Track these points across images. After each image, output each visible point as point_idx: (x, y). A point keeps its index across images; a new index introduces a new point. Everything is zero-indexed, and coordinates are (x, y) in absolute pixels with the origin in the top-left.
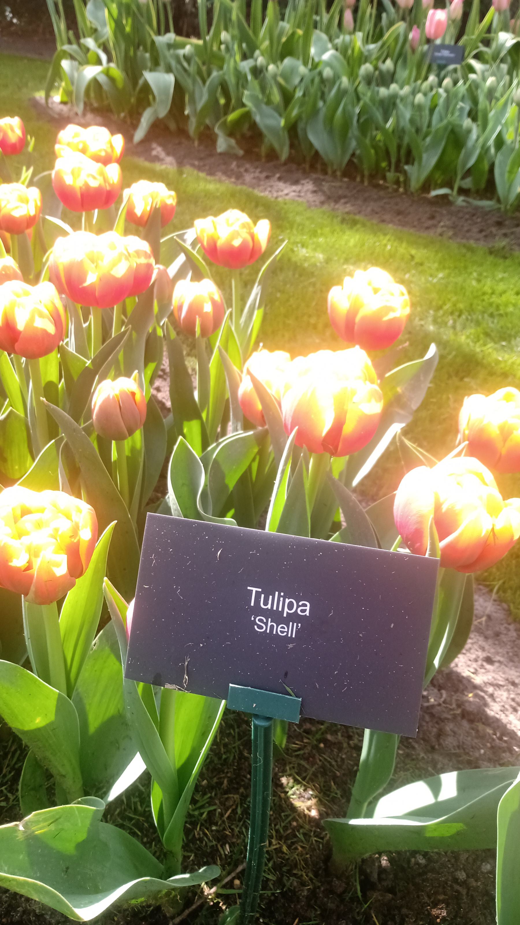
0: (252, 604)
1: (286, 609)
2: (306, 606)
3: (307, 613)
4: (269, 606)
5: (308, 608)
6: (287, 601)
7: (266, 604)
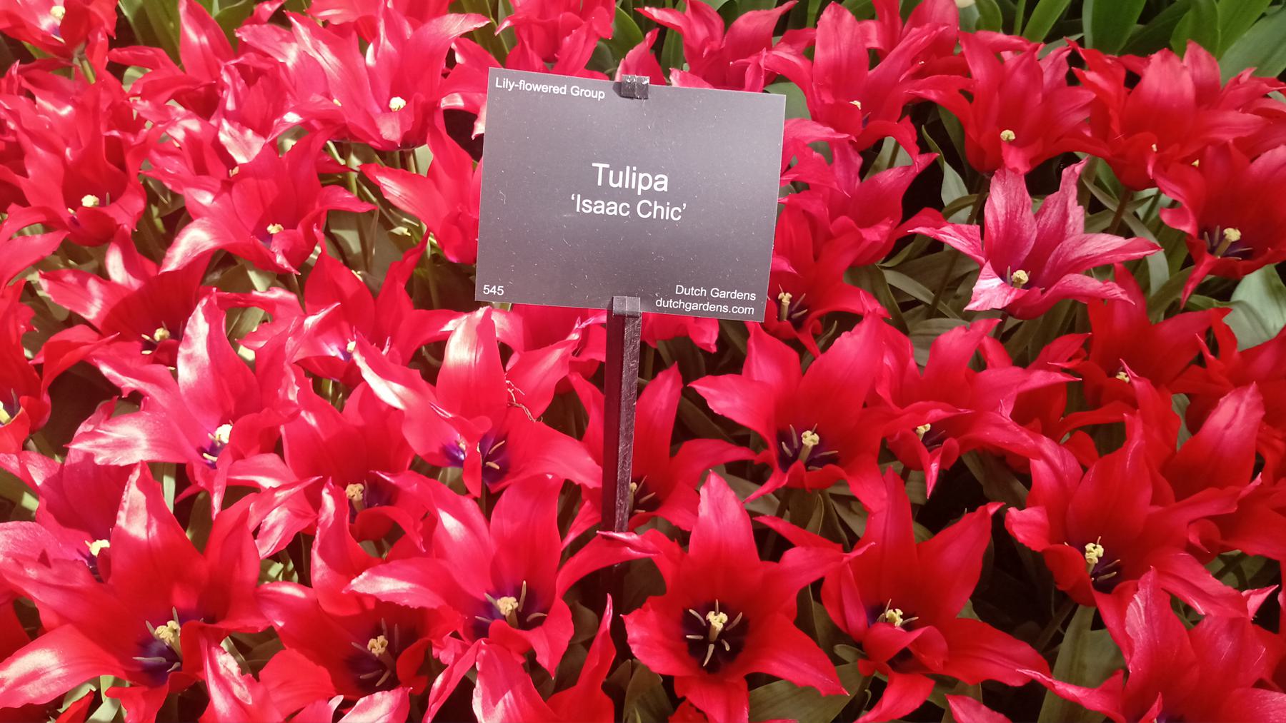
0: (600, 183)
1: (641, 187)
3: (665, 189)
4: (620, 184)
5: (665, 182)
7: (616, 181)
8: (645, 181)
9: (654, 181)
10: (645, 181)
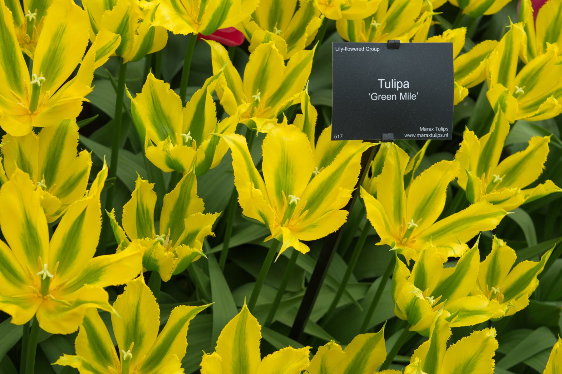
1: (398, 87)
2: (406, 83)
3: (408, 87)
5: (408, 84)
6: (398, 83)
7: (388, 86)
8: (400, 85)
9: (403, 84)
10: (400, 85)
